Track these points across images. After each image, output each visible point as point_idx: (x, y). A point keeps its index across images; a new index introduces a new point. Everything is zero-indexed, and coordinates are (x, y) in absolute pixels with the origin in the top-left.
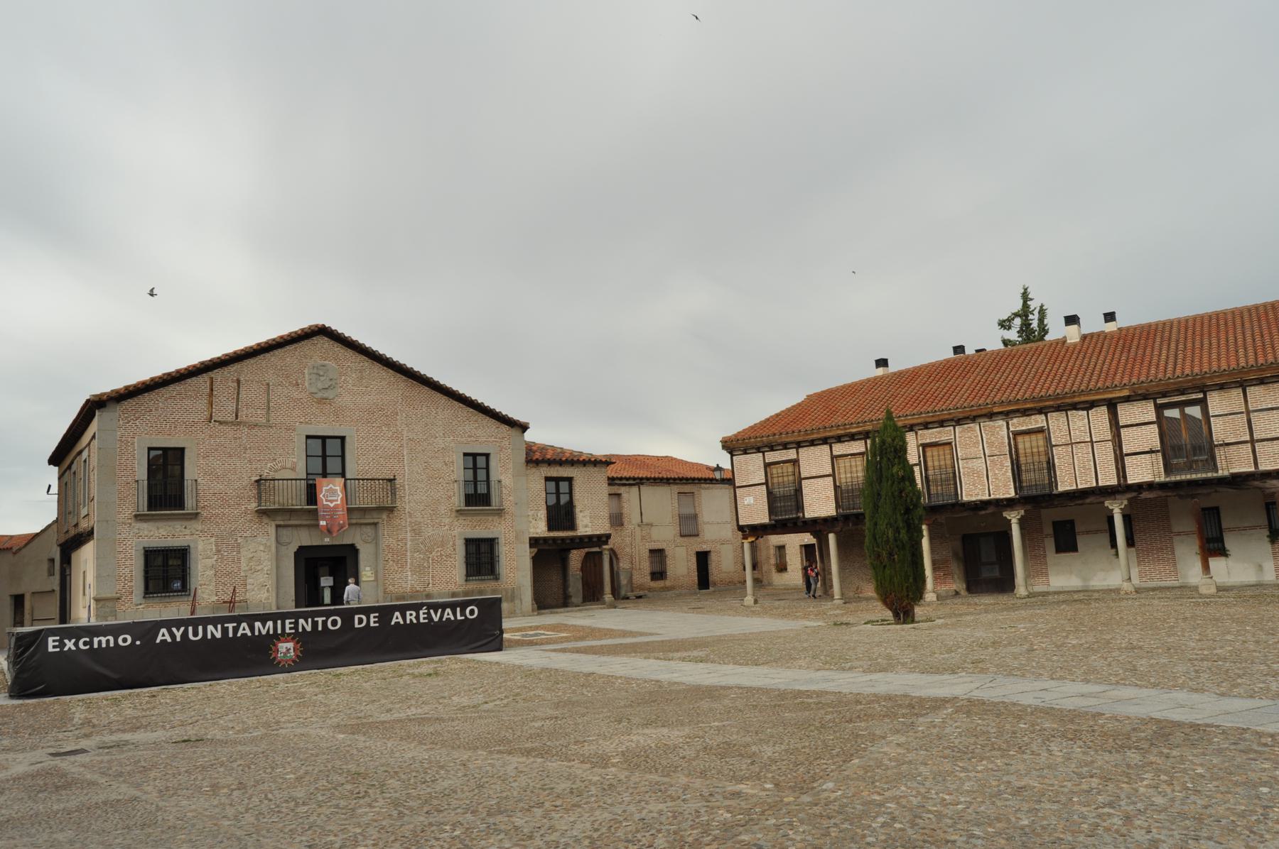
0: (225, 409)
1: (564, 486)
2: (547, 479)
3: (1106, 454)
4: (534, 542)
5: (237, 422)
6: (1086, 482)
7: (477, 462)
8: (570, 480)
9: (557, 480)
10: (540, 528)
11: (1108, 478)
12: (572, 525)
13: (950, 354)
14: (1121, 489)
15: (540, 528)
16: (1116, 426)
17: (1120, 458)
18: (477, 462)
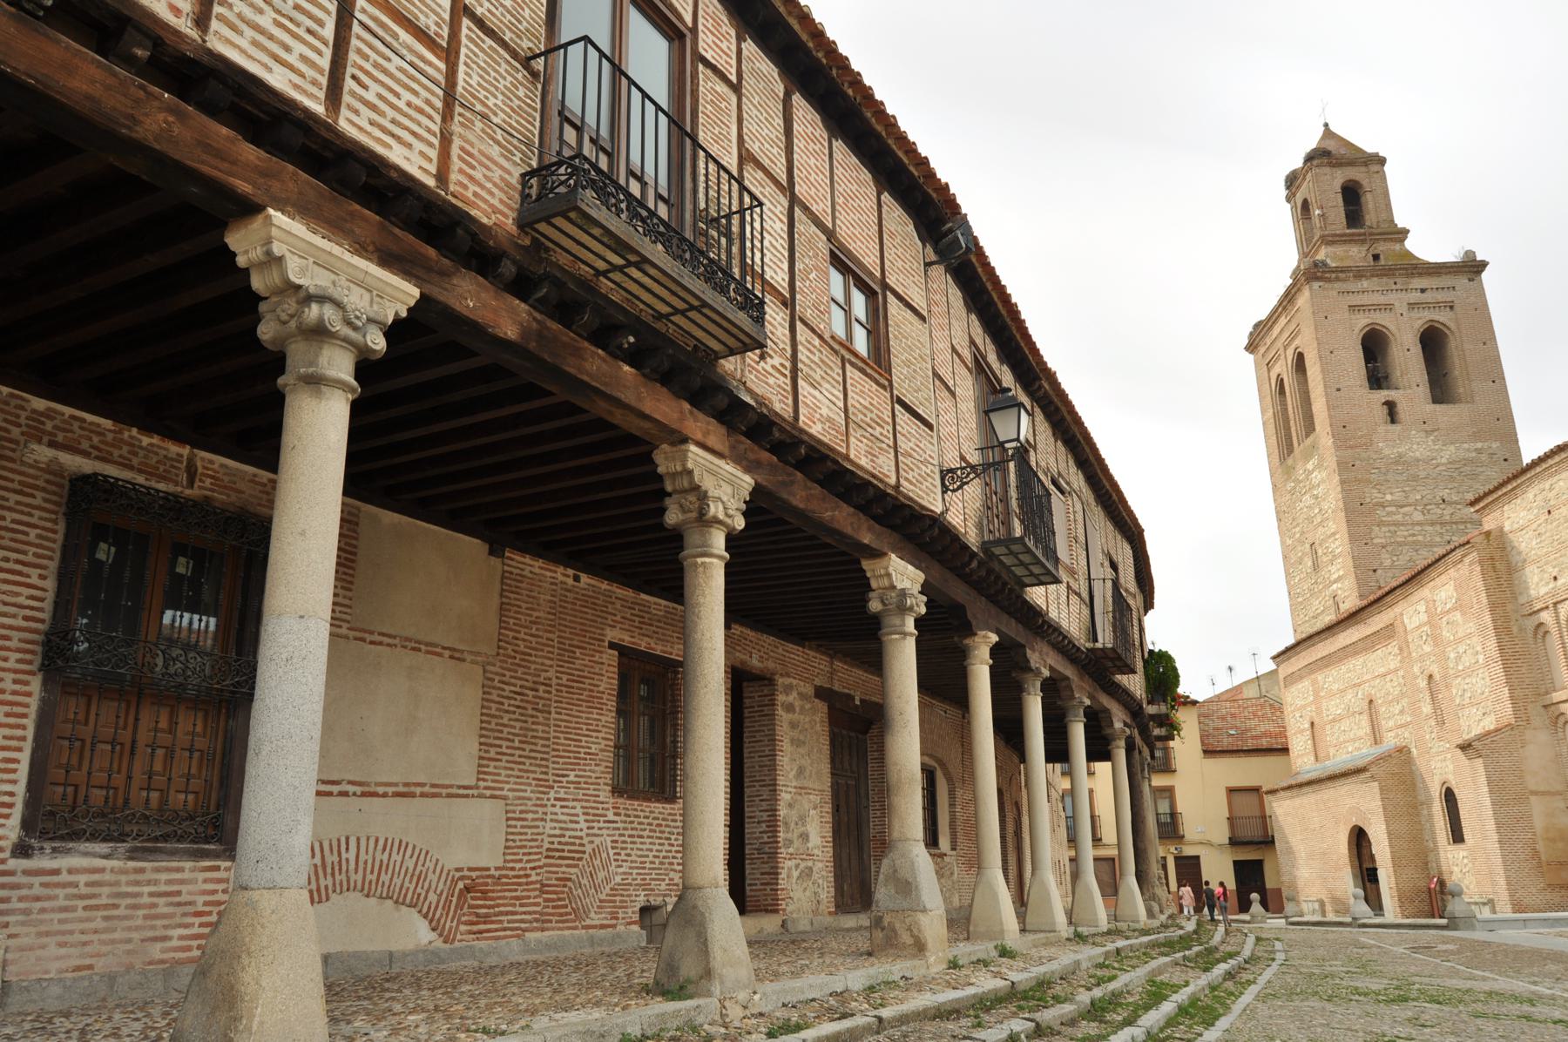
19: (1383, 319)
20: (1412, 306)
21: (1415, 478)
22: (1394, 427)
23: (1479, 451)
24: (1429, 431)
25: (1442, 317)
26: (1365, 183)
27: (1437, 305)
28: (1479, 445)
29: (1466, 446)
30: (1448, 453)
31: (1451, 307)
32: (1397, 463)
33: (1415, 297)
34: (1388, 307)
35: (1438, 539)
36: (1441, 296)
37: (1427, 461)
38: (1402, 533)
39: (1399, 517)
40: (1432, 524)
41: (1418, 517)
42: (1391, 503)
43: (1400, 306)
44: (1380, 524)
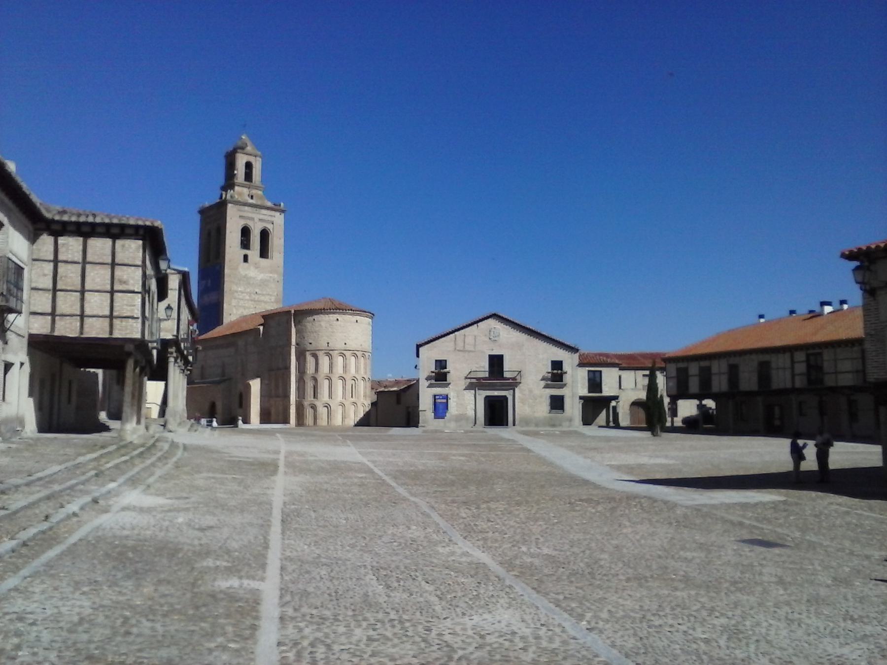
0: (460, 345)
1: (597, 375)
2: (589, 371)
3: (788, 374)
4: (581, 398)
5: (464, 351)
6: (782, 386)
7: (557, 365)
8: (601, 372)
9: (594, 372)
10: (584, 391)
11: (789, 385)
12: (601, 392)
13: (787, 313)
14: (794, 390)
15: (584, 391)
16: (793, 362)
17: (793, 376)
18: (557, 365)
19: (251, 224)
20: (260, 220)
21: (249, 284)
22: (245, 264)
23: (271, 277)
24: (257, 266)
25: (269, 226)
26: (253, 163)
27: (267, 221)
28: (271, 275)
29: (267, 275)
30: (261, 277)
31: (273, 224)
32: (244, 277)
33: (262, 217)
34: (252, 219)
35: (252, 306)
36: (270, 218)
37: (254, 278)
38: (241, 303)
39: (241, 297)
40: (252, 300)
41: (247, 297)
42: (240, 291)
43: (256, 220)
44: (235, 298)
